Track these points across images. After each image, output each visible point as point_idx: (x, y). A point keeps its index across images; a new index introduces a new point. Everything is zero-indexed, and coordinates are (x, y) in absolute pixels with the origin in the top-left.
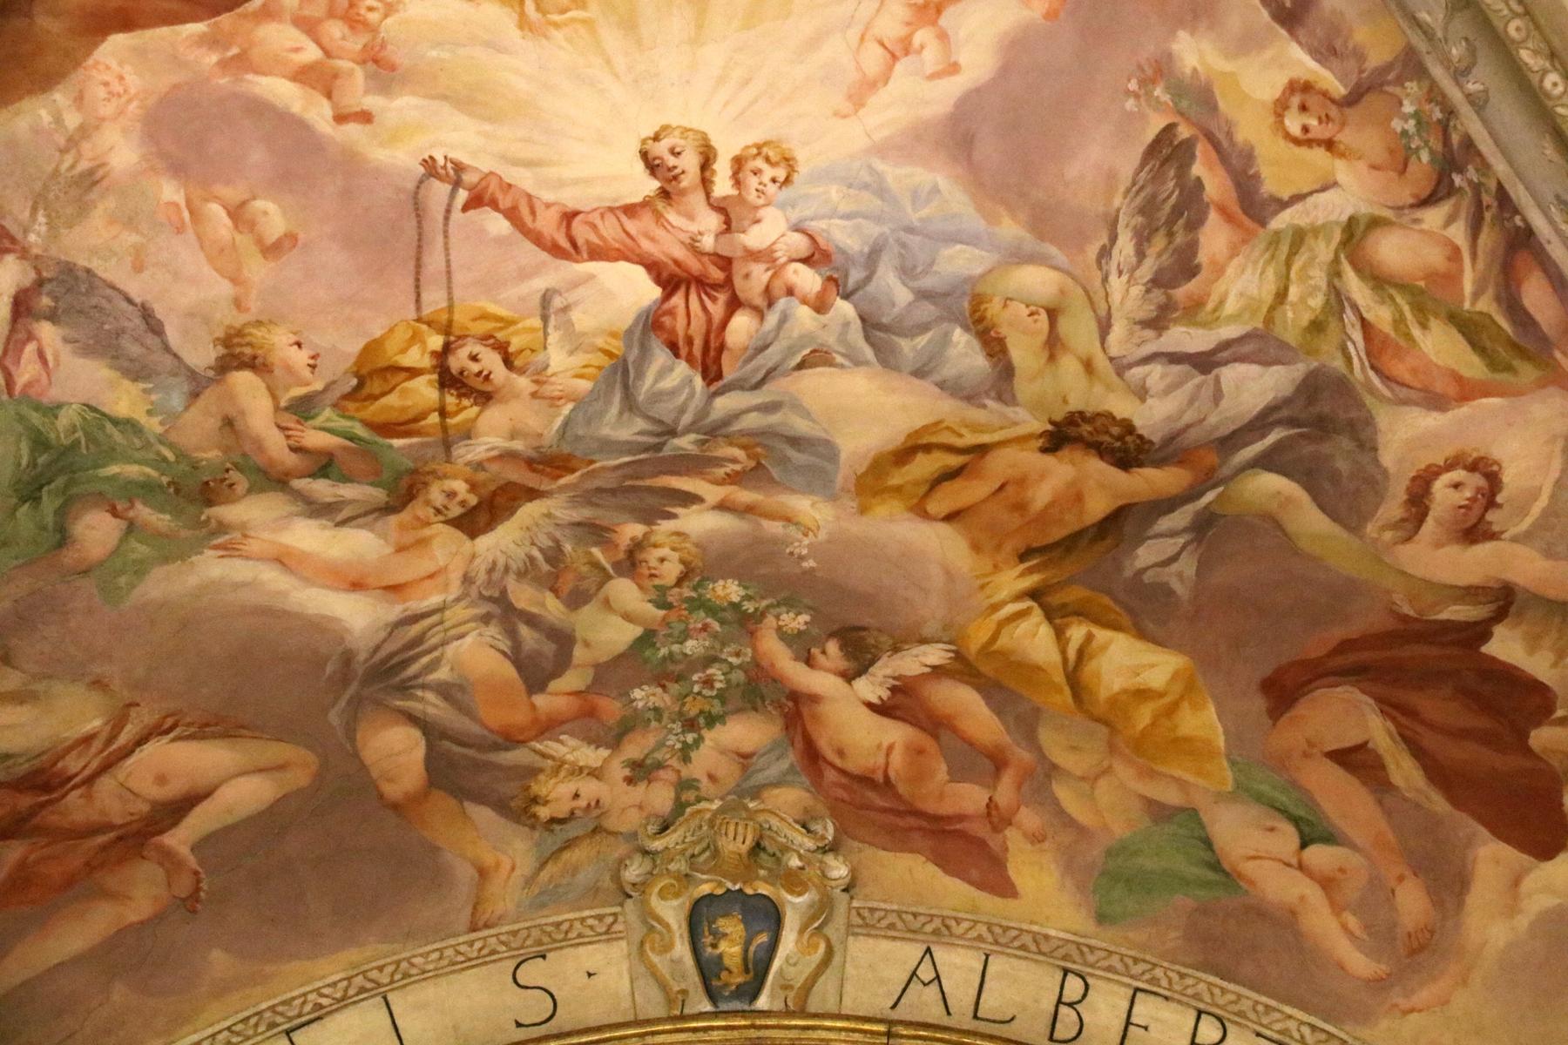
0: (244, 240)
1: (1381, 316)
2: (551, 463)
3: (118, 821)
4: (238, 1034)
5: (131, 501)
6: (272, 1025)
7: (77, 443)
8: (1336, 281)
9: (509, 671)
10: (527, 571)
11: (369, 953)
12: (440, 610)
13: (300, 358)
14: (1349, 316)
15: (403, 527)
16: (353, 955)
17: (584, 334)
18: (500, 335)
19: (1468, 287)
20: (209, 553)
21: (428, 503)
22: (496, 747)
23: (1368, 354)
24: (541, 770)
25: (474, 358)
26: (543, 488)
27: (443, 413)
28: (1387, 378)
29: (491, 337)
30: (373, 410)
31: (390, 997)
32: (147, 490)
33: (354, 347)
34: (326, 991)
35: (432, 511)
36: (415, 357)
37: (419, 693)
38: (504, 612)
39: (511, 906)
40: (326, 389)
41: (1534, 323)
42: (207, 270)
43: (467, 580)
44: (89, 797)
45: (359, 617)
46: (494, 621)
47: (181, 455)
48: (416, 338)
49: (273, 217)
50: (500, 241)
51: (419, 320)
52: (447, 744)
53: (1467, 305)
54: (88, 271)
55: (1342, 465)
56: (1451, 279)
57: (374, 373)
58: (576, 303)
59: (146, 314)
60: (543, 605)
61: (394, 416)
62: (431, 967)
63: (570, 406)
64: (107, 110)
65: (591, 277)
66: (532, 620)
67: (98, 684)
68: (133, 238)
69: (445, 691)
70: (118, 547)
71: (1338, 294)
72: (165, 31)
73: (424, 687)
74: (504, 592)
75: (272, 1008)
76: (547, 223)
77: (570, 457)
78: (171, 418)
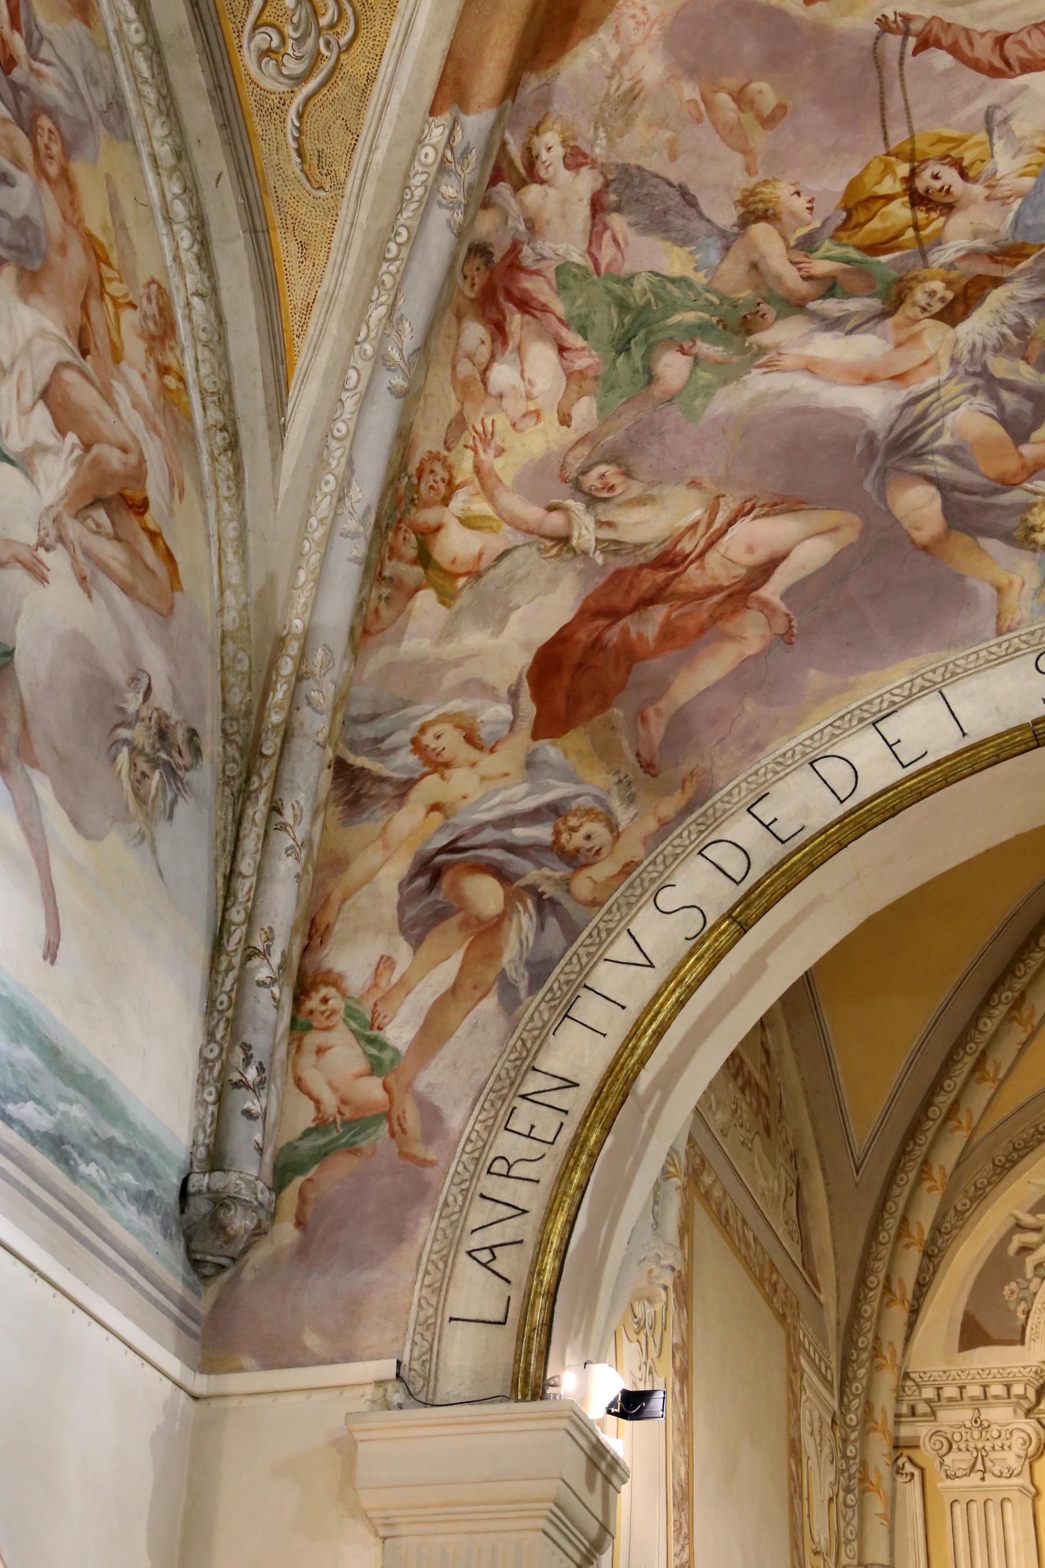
0: (748, 118)
2: (1010, 253)
3: (726, 584)
4: (838, 728)
5: (693, 341)
6: (862, 720)
7: (649, 302)
9: (998, 430)
10: (1001, 347)
11: (925, 661)
12: (937, 388)
13: (799, 204)
15: (897, 327)
16: (911, 663)
17: (1023, 138)
18: (954, 154)
20: (755, 371)
21: (915, 304)
22: (996, 492)
24: (1035, 505)
25: (936, 177)
26: (1005, 275)
27: (916, 227)
29: (948, 156)
30: (861, 236)
31: (944, 691)
32: (701, 330)
33: (841, 186)
34: (896, 691)
35: (918, 310)
36: (889, 186)
37: (930, 458)
38: (987, 383)
39: (1026, 613)
42: (723, 148)
43: (954, 361)
44: (702, 568)
45: (875, 405)
46: (980, 391)
47: (723, 299)
48: (888, 169)
49: (766, 94)
50: (947, 74)
51: (888, 154)
52: (957, 495)
54: (638, 168)
57: (859, 205)
58: (1014, 114)
59: (683, 192)
60: (1017, 371)
61: (880, 238)
62: (971, 666)
63: (1019, 201)
64: (636, 38)
65: (1024, 88)
66: (1011, 386)
67: (694, 484)
68: (666, 135)
69: (950, 453)
70: (690, 377)
73: (932, 452)
74: (985, 366)
75: (859, 707)
76: (983, 49)
77: (1024, 245)
78: (713, 271)
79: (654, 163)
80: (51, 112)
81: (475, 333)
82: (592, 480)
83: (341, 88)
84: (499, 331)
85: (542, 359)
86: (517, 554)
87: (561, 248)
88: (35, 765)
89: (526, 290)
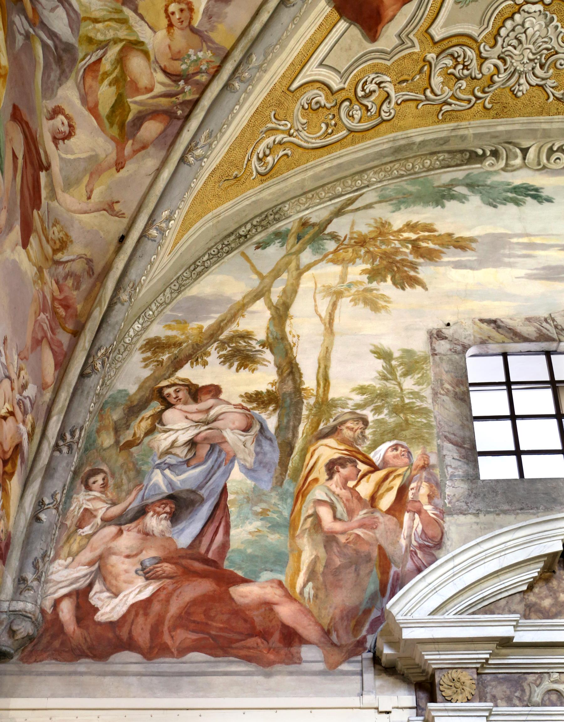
1: (106, 65)
8: (112, 42)
14: (100, 52)
19: (138, 98)
23: (89, 66)
28: (84, 77)
41: (139, 129)
53: (129, 100)
55: (52, 75)
56: (137, 90)
71: (107, 45)
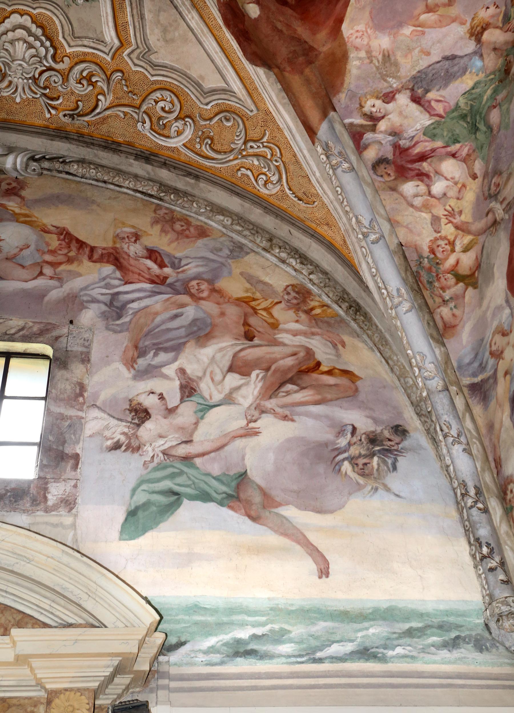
40: (506, 6)
42: (444, 30)
54: (419, 72)
68: (416, 51)
72: (349, 9)
79: (424, 63)
80: (197, 277)
81: (409, 188)
82: (493, 188)
83: (291, 168)
84: (422, 176)
85: (450, 167)
86: (486, 244)
87: (418, 126)
88: (280, 505)
89: (418, 153)
